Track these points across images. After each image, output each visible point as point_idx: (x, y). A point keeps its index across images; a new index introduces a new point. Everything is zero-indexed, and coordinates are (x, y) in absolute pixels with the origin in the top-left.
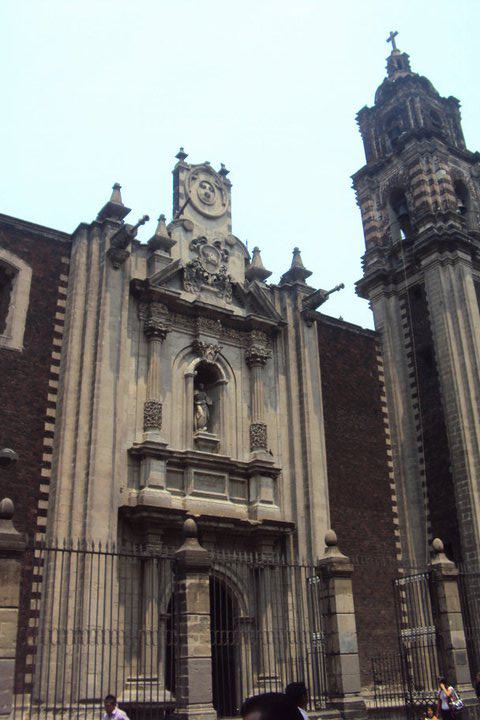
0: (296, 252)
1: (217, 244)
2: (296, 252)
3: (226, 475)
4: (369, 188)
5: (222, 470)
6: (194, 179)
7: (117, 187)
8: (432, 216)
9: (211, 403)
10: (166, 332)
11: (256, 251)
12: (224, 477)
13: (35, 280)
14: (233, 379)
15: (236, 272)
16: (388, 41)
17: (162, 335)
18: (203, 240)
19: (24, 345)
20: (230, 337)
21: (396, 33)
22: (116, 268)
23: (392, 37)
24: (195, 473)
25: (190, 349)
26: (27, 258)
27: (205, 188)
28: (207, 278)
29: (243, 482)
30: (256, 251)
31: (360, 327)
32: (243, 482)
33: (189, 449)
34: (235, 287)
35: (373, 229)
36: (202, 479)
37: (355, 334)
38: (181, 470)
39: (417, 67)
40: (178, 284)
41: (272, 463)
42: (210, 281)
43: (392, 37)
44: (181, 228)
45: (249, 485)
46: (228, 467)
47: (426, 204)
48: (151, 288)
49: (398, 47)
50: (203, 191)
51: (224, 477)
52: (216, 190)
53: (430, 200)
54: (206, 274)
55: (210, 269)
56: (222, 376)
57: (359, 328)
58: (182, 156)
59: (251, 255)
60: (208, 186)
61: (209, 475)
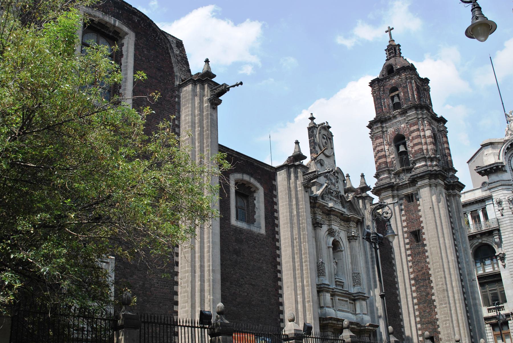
0: (363, 176)
2: (363, 176)
4: (382, 131)
5: (346, 297)
8: (425, 158)
10: (321, 224)
16: (386, 32)
21: (393, 29)
23: (390, 30)
24: (339, 299)
29: (352, 303)
32: (352, 303)
39: (409, 56)
43: (390, 30)
47: (422, 149)
49: (393, 38)
53: (424, 147)
61: (342, 300)
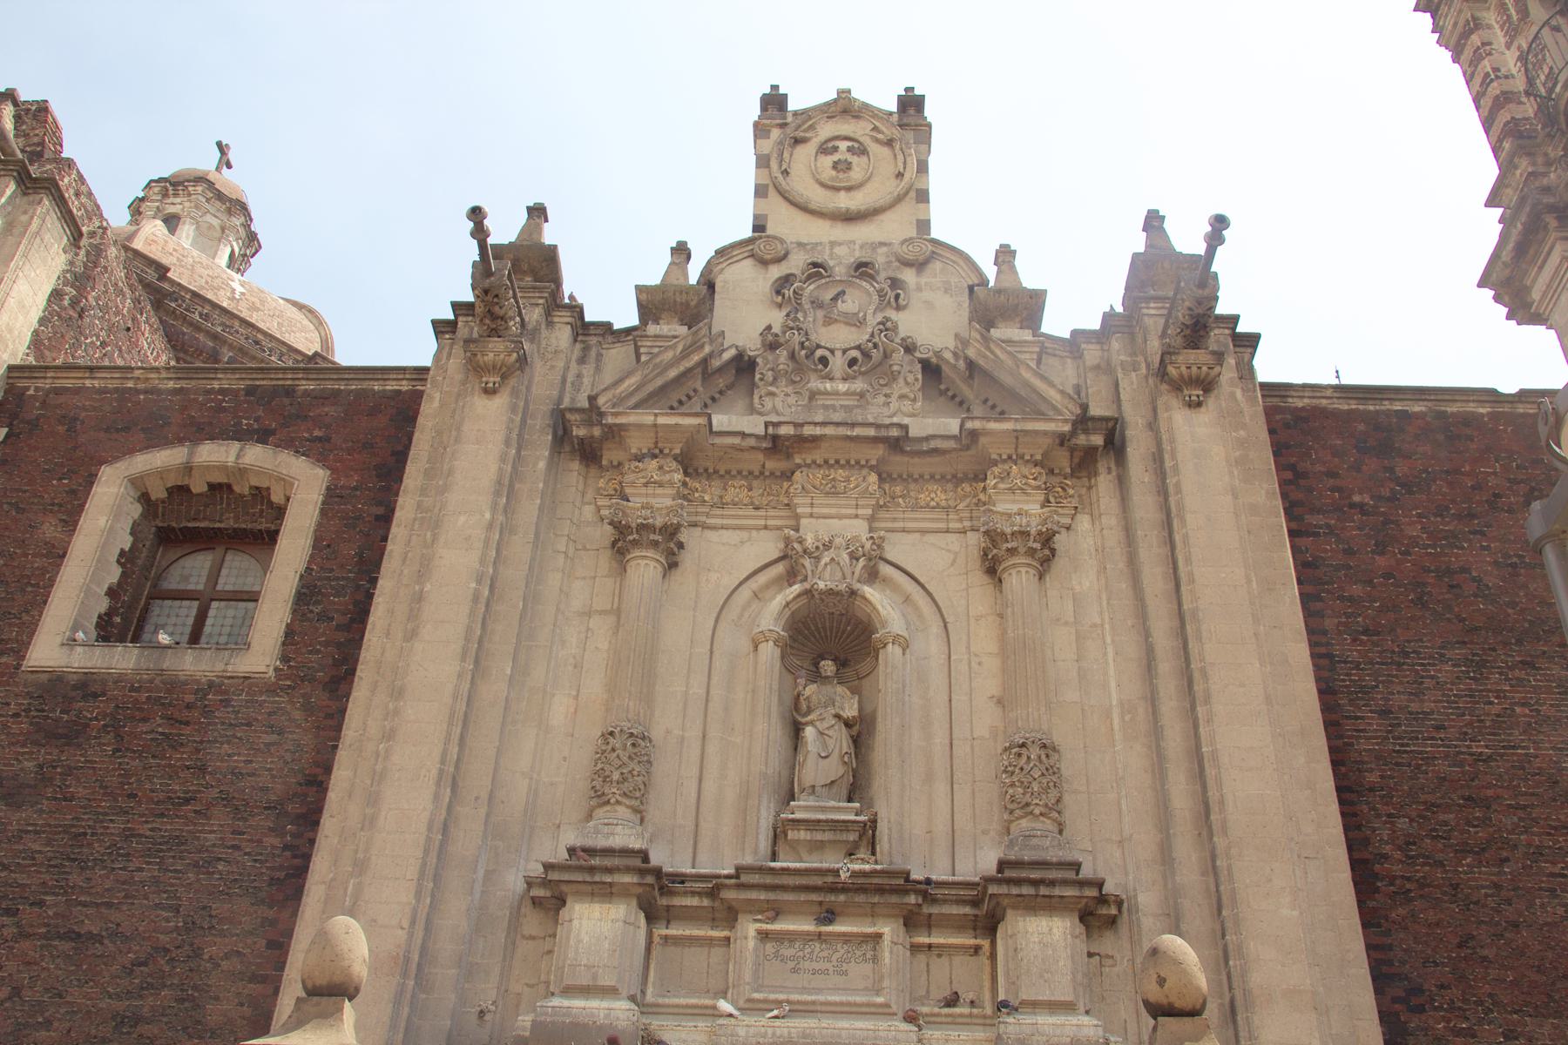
1: (863, 269)
3: (889, 930)
5: (873, 913)
6: (797, 141)
7: (537, 213)
9: (850, 711)
11: (1005, 256)
12: (879, 936)
13: (332, 496)
14: (935, 628)
15: (933, 322)
17: (669, 544)
18: (817, 270)
19: (285, 658)
20: (916, 507)
22: (490, 392)
25: (780, 568)
26: (317, 450)
27: (836, 149)
28: (824, 361)
30: (1005, 256)
31: (1493, 393)
32: (977, 950)
33: (748, 860)
34: (931, 370)
35: (1505, 98)
36: (788, 952)
37: (1467, 420)
38: (725, 933)
40: (741, 404)
41: (1076, 866)
42: (838, 363)
44: (749, 262)
45: (993, 956)
46: (912, 900)
48: (610, 420)
50: (827, 161)
51: (879, 936)
52: (874, 148)
54: (819, 353)
55: (838, 338)
56: (884, 624)
57: (1491, 395)
58: (774, 102)
59: (990, 272)
60: (843, 145)
